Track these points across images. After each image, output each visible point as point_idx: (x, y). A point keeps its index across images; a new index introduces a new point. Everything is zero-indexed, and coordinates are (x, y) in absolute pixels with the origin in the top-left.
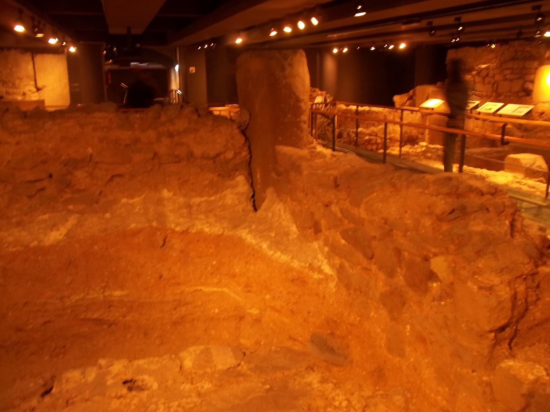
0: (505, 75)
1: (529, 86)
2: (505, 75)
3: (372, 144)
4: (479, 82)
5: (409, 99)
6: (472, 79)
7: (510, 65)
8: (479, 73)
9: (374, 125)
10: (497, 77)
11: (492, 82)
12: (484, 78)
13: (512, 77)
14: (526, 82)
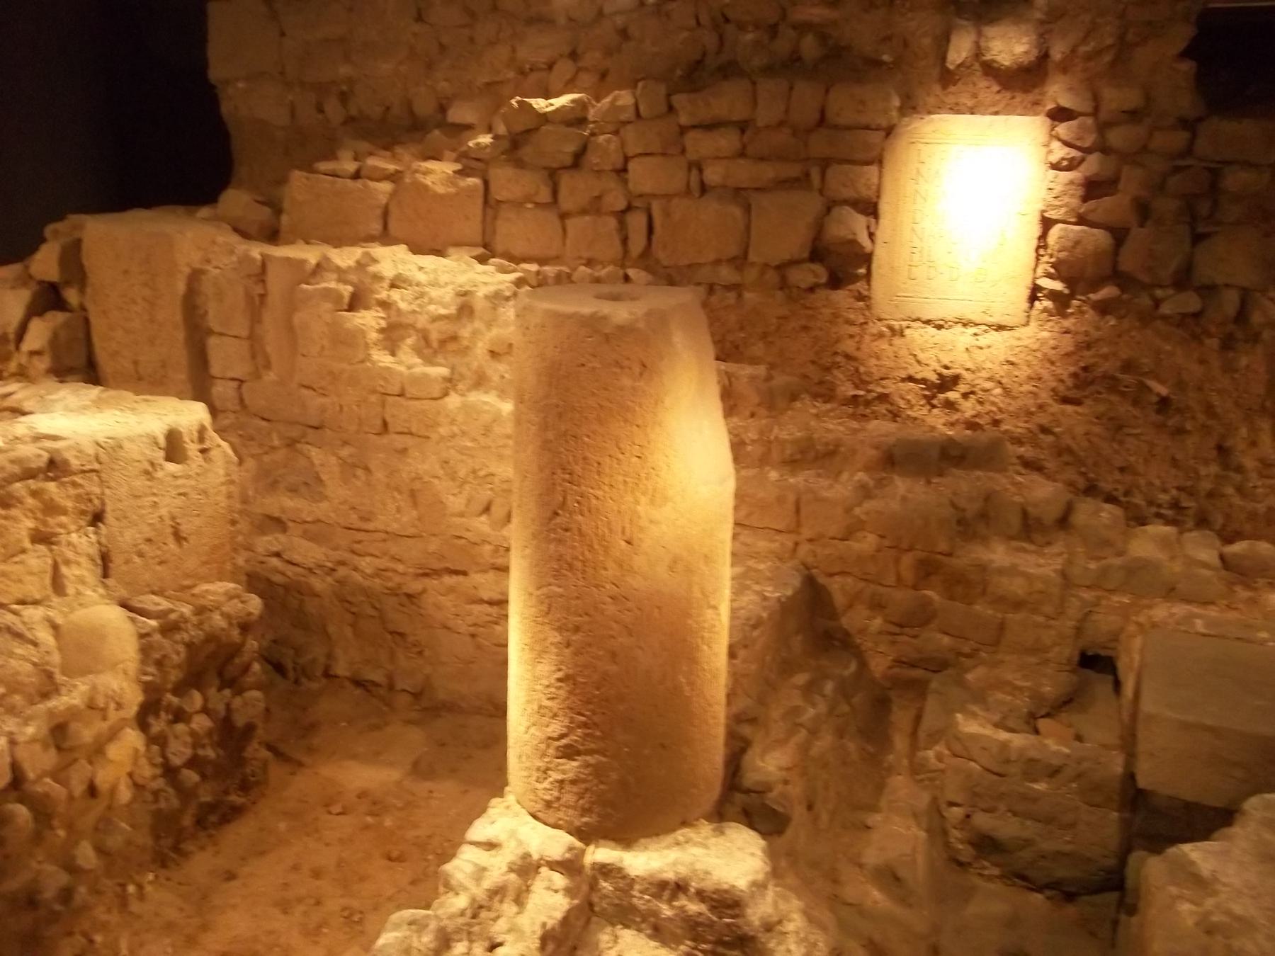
0: (697, 166)
2: (697, 166)
4: (518, 204)
10: (643, 176)
12: (553, 175)
13: (744, 173)
14: (831, 206)
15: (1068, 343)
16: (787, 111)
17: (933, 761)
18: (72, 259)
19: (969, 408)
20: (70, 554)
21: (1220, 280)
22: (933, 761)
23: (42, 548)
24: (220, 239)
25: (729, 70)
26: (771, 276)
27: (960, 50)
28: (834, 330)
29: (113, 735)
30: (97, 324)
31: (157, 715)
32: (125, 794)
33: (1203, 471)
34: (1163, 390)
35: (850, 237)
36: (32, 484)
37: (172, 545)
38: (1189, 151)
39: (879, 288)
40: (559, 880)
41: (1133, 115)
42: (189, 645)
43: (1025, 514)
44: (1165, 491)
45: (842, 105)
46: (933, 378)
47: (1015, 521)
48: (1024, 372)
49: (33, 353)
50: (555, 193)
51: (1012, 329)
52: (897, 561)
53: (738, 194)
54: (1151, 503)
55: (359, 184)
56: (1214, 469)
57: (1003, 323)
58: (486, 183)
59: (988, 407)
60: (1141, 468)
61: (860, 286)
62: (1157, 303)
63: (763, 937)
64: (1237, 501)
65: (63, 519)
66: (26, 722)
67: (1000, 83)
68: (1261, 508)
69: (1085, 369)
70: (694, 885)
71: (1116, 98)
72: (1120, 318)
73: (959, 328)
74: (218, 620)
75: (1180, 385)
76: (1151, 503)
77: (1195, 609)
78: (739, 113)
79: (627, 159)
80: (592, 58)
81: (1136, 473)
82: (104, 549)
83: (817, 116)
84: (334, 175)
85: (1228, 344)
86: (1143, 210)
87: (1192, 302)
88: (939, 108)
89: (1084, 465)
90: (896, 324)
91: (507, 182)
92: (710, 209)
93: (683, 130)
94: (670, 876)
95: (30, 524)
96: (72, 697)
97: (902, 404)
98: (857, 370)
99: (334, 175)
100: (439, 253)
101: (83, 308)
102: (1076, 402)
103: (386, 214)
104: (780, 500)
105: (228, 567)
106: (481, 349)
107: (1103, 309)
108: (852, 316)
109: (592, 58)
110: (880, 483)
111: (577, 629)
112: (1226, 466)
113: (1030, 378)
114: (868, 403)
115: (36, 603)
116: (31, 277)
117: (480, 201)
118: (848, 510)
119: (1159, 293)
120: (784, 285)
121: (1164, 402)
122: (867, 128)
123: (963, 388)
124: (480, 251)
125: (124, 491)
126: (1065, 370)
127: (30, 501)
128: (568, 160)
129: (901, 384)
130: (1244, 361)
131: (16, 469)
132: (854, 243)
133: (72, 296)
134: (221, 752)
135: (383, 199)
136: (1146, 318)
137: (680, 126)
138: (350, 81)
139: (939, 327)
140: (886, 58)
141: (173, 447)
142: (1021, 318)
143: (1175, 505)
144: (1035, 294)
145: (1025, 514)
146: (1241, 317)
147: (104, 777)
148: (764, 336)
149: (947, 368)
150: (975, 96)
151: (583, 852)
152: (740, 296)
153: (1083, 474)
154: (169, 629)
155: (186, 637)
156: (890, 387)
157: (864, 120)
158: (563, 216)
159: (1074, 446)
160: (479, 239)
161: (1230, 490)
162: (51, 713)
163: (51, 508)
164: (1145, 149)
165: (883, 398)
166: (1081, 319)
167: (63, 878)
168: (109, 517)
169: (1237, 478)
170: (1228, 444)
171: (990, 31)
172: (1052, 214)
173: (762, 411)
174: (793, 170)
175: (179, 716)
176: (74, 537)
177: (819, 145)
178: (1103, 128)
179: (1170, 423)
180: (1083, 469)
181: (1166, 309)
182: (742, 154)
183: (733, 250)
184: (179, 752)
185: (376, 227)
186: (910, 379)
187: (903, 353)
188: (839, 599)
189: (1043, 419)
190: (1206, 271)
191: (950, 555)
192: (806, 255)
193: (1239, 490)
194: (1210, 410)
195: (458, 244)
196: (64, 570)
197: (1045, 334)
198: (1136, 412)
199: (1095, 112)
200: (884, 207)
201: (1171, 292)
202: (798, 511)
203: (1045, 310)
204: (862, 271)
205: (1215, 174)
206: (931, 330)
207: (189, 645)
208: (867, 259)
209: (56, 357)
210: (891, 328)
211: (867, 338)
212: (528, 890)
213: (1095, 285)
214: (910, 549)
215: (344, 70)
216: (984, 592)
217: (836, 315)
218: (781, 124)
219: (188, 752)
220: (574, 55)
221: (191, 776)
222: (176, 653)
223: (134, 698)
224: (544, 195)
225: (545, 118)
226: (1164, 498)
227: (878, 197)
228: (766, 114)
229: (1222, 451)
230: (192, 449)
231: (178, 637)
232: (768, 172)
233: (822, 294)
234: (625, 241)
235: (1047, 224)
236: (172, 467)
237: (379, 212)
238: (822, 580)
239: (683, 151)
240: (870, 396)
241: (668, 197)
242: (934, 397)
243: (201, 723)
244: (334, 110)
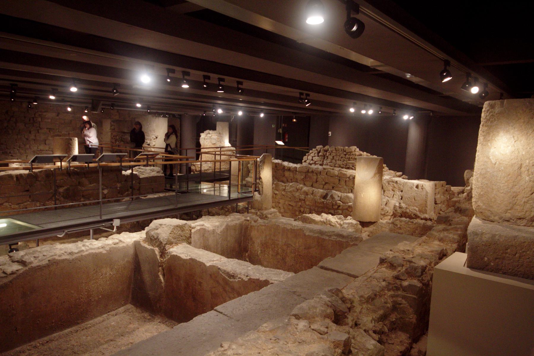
20: (396, 194)
23: (393, 192)
29: (388, 215)
36: (393, 183)
42: (402, 212)
74: (408, 211)
95: (392, 188)
125: (406, 189)
127: (392, 185)
141: (417, 187)
154: (400, 207)
163: (394, 187)
168: (403, 191)
176: (398, 192)
196: (394, 195)
207: (402, 212)
222: (399, 211)
230: (420, 188)
236: (416, 189)
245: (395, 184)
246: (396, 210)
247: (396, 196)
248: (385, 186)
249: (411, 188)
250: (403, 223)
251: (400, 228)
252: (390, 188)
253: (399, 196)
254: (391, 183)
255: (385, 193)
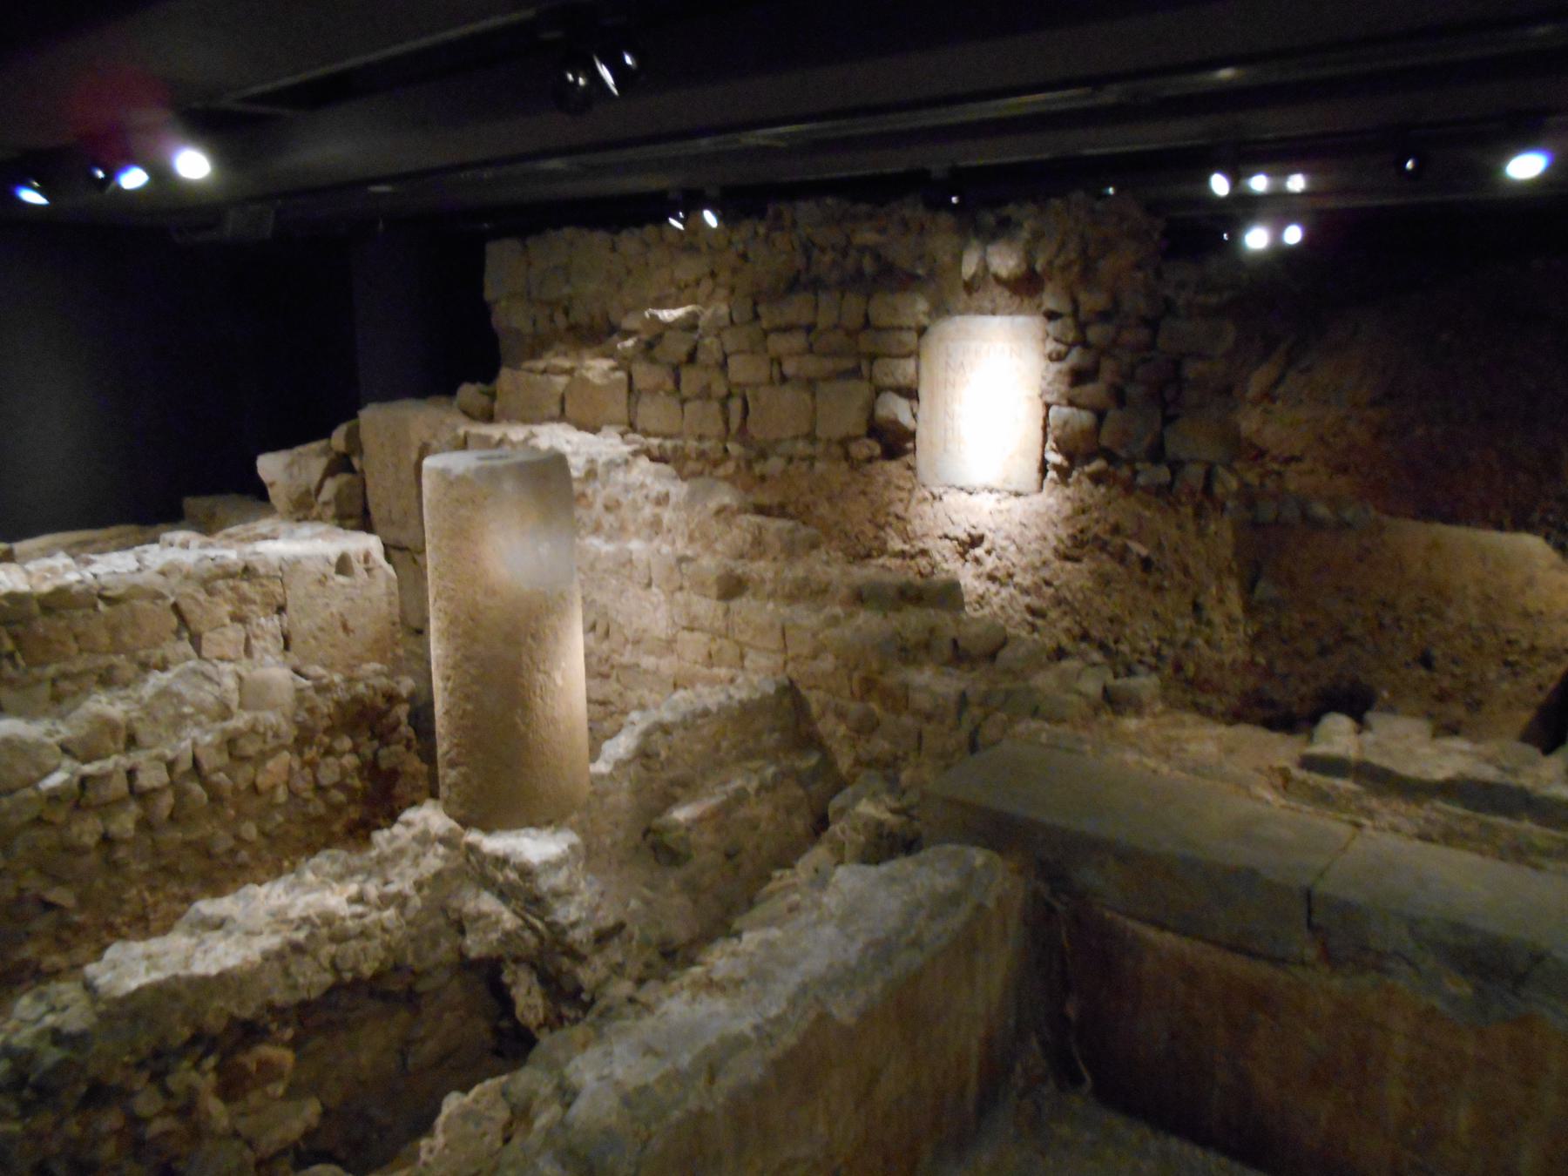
0: (777, 361)
1: (899, 409)
2: (777, 361)
3: (106, 809)
4: (654, 391)
5: (330, 472)
6: (620, 375)
7: (797, 309)
8: (649, 348)
9: (107, 680)
10: (741, 369)
11: (720, 389)
13: (812, 366)
14: (879, 391)
15: (1067, 508)
16: (840, 317)
17: (839, 833)
18: (353, 437)
19: (990, 563)
20: (258, 632)
21: (1183, 455)
22: (839, 833)
23: (239, 626)
24: (448, 421)
25: (816, 285)
26: (836, 450)
27: (970, 266)
28: (887, 494)
29: (275, 752)
30: (370, 482)
31: (311, 748)
32: (281, 795)
33: (1179, 623)
34: (1144, 552)
35: (892, 417)
36: (231, 582)
37: (341, 633)
38: (1151, 346)
39: (922, 460)
40: (441, 850)
41: (1104, 316)
42: (338, 704)
43: (955, 642)
44: (1147, 640)
45: (880, 311)
46: (964, 536)
47: (947, 651)
48: (1032, 533)
49: (326, 504)
50: (677, 382)
51: (1027, 495)
52: (850, 679)
53: (810, 383)
54: (1134, 650)
55: (545, 377)
56: (1188, 622)
57: (1020, 490)
58: (630, 377)
59: (1005, 562)
60: (1128, 620)
61: (908, 458)
62: (1135, 473)
63: (549, 899)
64: (1207, 652)
65: (254, 608)
66: (207, 732)
67: (1010, 290)
68: (1228, 659)
69: (1082, 531)
70: (512, 861)
71: (1092, 301)
72: (1109, 488)
73: (986, 494)
74: (361, 687)
75: (1159, 547)
76: (1134, 650)
77: (1047, 726)
78: (806, 317)
79: (726, 357)
80: (724, 276)
81: (1123, 624)
82: (286, 632)
83: (862, 320)
84: (531, 371)
85: (1199, 513)
86: (1119, 396)
87: (1163, 474)
88: (966, 311)
89: (1079, 614)
90: (936, 491)
91: (646, 375)
92: (788, 394)
93: (766, 333)
94: (500, 853)
96: (240, 721)
97: (938, 558)
98: (905, 529)
99: (531, 371)
100: (595, 430)
101: (362, 471)
102: (1077, 560)
103: (563, 400)
104: (772, 626)
105: (389, 655)
106: (599, 505)
107: (1096, 479)
108: (901, 483)
109: (724, 276)
110: (850, 616)
111: (448, 678)
112: (1199, 620)
113: (1037, 538)
114: (912, 557)
115: (230, 661)
116: (331, 449)
117: (624, 391)
118: (814, 635)
119: (1139, 466)
120: (847, 456)
121: (1146, 564)
122: (900, 328)
123: (986, 545)
124: (622, 428)
125: (301, 592)
126: (1064, 532)
127: (229, 593)
128: (684, 358)
129: (938, 541)
130: (1212, 527)
131: (220, 572)
132: (896, 422)
133: (356, 462)
134: (368, 784)
135: (560, 389)
136: (1129, 488)
137: (763, 329)
138: (570, 298)
139: (971, 494)
140: (920, 272)
141: (343, 565)
142: (1034, 486)
143: (1157, 653)
144: (1043, 468)
145: (955, 642)
146: (1208, 489)
147: (263, 781)
148: (830, 499)
149: (974, 527)
150: (993, 301)
151: (462, 835)
152: (812, 465)
153: (1080, 624)
154: (322, 688)
155: (335, 696)
156: (929, 544)
157: (896, 322)
158: (683, 401)
159: (1069, 597)
160: (626, 419)
161: (1199, 642)
162: (223, 731)
163: (244, 599)
164: (1114, 342)
165: (924, 553)
166: (1081, 487)
167: (231, 843)
168: (290, 609)
169: (1207, 631)
170: (1201, 599)
171: (991, 249)
172: (1049, 398)
173: (782, 557)
174: (848, 363)
175: (329, 751)
176: (263, 620)
177: (865, 342)
178: (1081, 327)
179: (1151, 580)
180: (1078, 618)
181: (1141, 480)
182: (810, 350)
183: (805, 428)
184: (328, 774)
185: (555, 410)
186: (946, 537)
187: (941, 515)
188: (815, 709)
189: (1046, 574)
190: (1175, 446)
191: (881, 673)
192: (862, 430)
193: (1208, 642)
194: (1186, 570)
195: (610, 423)
196: (253, 641)
197: (1051, 501)
198: (1120, 569)
199: (1075, 312)
200: (923, 393)
201: (1148, 465)
202: (784, 634)
203: (1052, 480)
204: (910, 445)
205: (1177, 364)
206: (964, 495)
207: (338, 704)
208: (912, 435)
209: (339, 506)
210: (932, 494)
211: (914, 502)
212: (424, 854)
213: (1088, 458)
214: (856, 667)
215: (566, 290)
216: (907, 708)
217: (888, 483)
218: (836, 327)
219: (337, 778)
220: (713, 274)
221: (339, 796)
222: (325, 705)
223: (289, 732)
224: (670, 385)
225: (668, 326)
226: (1144, 645)
227: (918, 383)
228: (823, 321)
229: (1197, 608)
230: (359, 567)
231: (329, 695)
232: (829, 365)
233: (879, 464)
234: (727, 422)
235: (1048, 406)
236: (341, 579)
237: (557, 399)
238: (804, 692)
239: (766, 351)
240: (913, 551)
241: (757, 385)
242: (966, 552)
243: (350, 761)
244: (561, 321)
245: (245, 586)
246: (311, 711)
247: (262, 643)
248: (198, 611)
249: (322, 581)
250: (678, 734)
251: (669, 761)
252: (224, 610)
253: (275, 637)
254: (221, 584)
255: (205, 644)
